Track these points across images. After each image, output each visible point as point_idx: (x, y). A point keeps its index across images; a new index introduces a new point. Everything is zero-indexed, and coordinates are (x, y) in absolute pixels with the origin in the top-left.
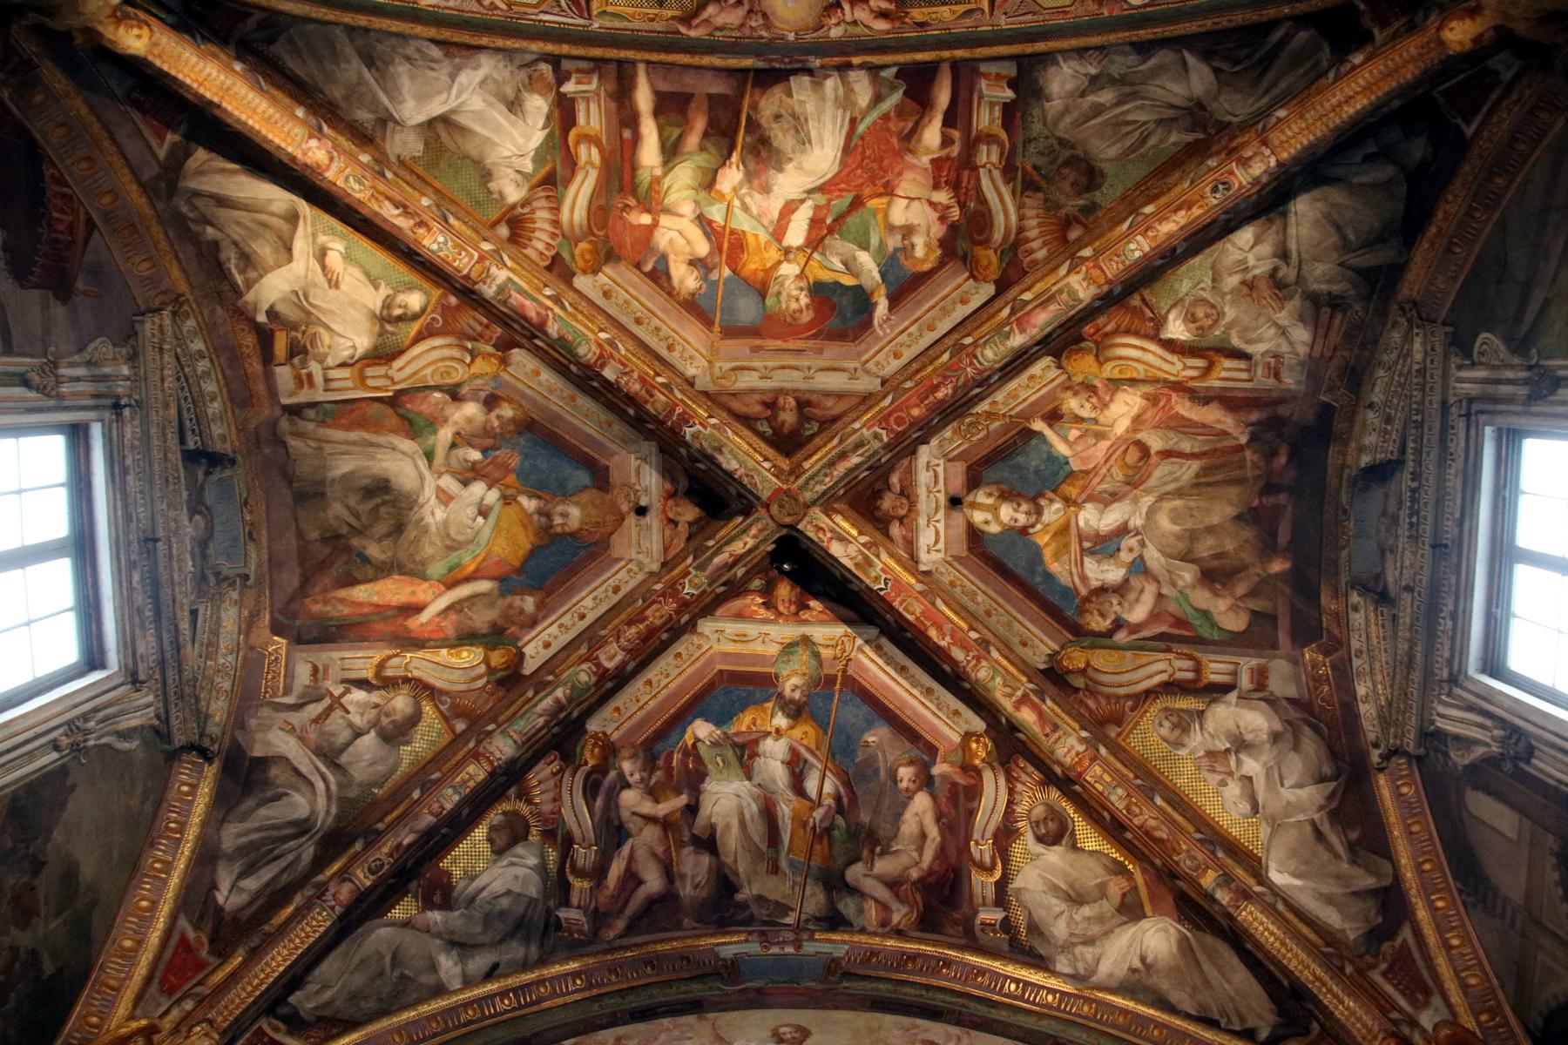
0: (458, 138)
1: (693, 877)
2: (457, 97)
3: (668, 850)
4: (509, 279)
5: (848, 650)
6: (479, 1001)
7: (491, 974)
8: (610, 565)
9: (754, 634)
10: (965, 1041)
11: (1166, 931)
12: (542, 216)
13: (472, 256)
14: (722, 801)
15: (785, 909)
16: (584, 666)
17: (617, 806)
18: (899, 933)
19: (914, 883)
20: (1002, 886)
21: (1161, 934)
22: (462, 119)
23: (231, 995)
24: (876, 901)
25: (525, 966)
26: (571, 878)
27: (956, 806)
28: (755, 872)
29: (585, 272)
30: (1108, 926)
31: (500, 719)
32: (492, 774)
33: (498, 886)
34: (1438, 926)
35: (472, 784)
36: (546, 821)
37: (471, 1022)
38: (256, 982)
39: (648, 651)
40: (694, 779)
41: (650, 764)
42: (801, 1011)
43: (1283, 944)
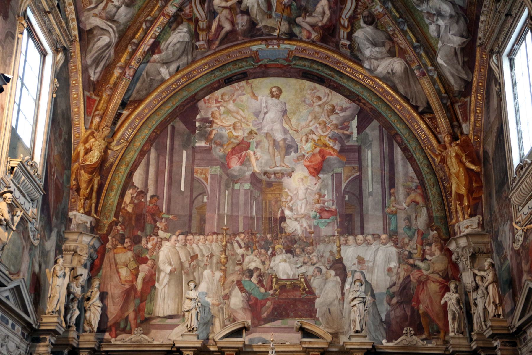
1: (241, 23)
3: (232, 17)
10: (330, 97)
11: (401, 64)
15: (274, 29)
18: (313, 43)
19: (320, 27)
21: (400, 64)
24: (306, 29)
25: (188, 65)
27: (337, 5)
30: (383, 56)
33: (175, 41)
34: (476, 104)
37: (175, 89)
43: (430, 94)
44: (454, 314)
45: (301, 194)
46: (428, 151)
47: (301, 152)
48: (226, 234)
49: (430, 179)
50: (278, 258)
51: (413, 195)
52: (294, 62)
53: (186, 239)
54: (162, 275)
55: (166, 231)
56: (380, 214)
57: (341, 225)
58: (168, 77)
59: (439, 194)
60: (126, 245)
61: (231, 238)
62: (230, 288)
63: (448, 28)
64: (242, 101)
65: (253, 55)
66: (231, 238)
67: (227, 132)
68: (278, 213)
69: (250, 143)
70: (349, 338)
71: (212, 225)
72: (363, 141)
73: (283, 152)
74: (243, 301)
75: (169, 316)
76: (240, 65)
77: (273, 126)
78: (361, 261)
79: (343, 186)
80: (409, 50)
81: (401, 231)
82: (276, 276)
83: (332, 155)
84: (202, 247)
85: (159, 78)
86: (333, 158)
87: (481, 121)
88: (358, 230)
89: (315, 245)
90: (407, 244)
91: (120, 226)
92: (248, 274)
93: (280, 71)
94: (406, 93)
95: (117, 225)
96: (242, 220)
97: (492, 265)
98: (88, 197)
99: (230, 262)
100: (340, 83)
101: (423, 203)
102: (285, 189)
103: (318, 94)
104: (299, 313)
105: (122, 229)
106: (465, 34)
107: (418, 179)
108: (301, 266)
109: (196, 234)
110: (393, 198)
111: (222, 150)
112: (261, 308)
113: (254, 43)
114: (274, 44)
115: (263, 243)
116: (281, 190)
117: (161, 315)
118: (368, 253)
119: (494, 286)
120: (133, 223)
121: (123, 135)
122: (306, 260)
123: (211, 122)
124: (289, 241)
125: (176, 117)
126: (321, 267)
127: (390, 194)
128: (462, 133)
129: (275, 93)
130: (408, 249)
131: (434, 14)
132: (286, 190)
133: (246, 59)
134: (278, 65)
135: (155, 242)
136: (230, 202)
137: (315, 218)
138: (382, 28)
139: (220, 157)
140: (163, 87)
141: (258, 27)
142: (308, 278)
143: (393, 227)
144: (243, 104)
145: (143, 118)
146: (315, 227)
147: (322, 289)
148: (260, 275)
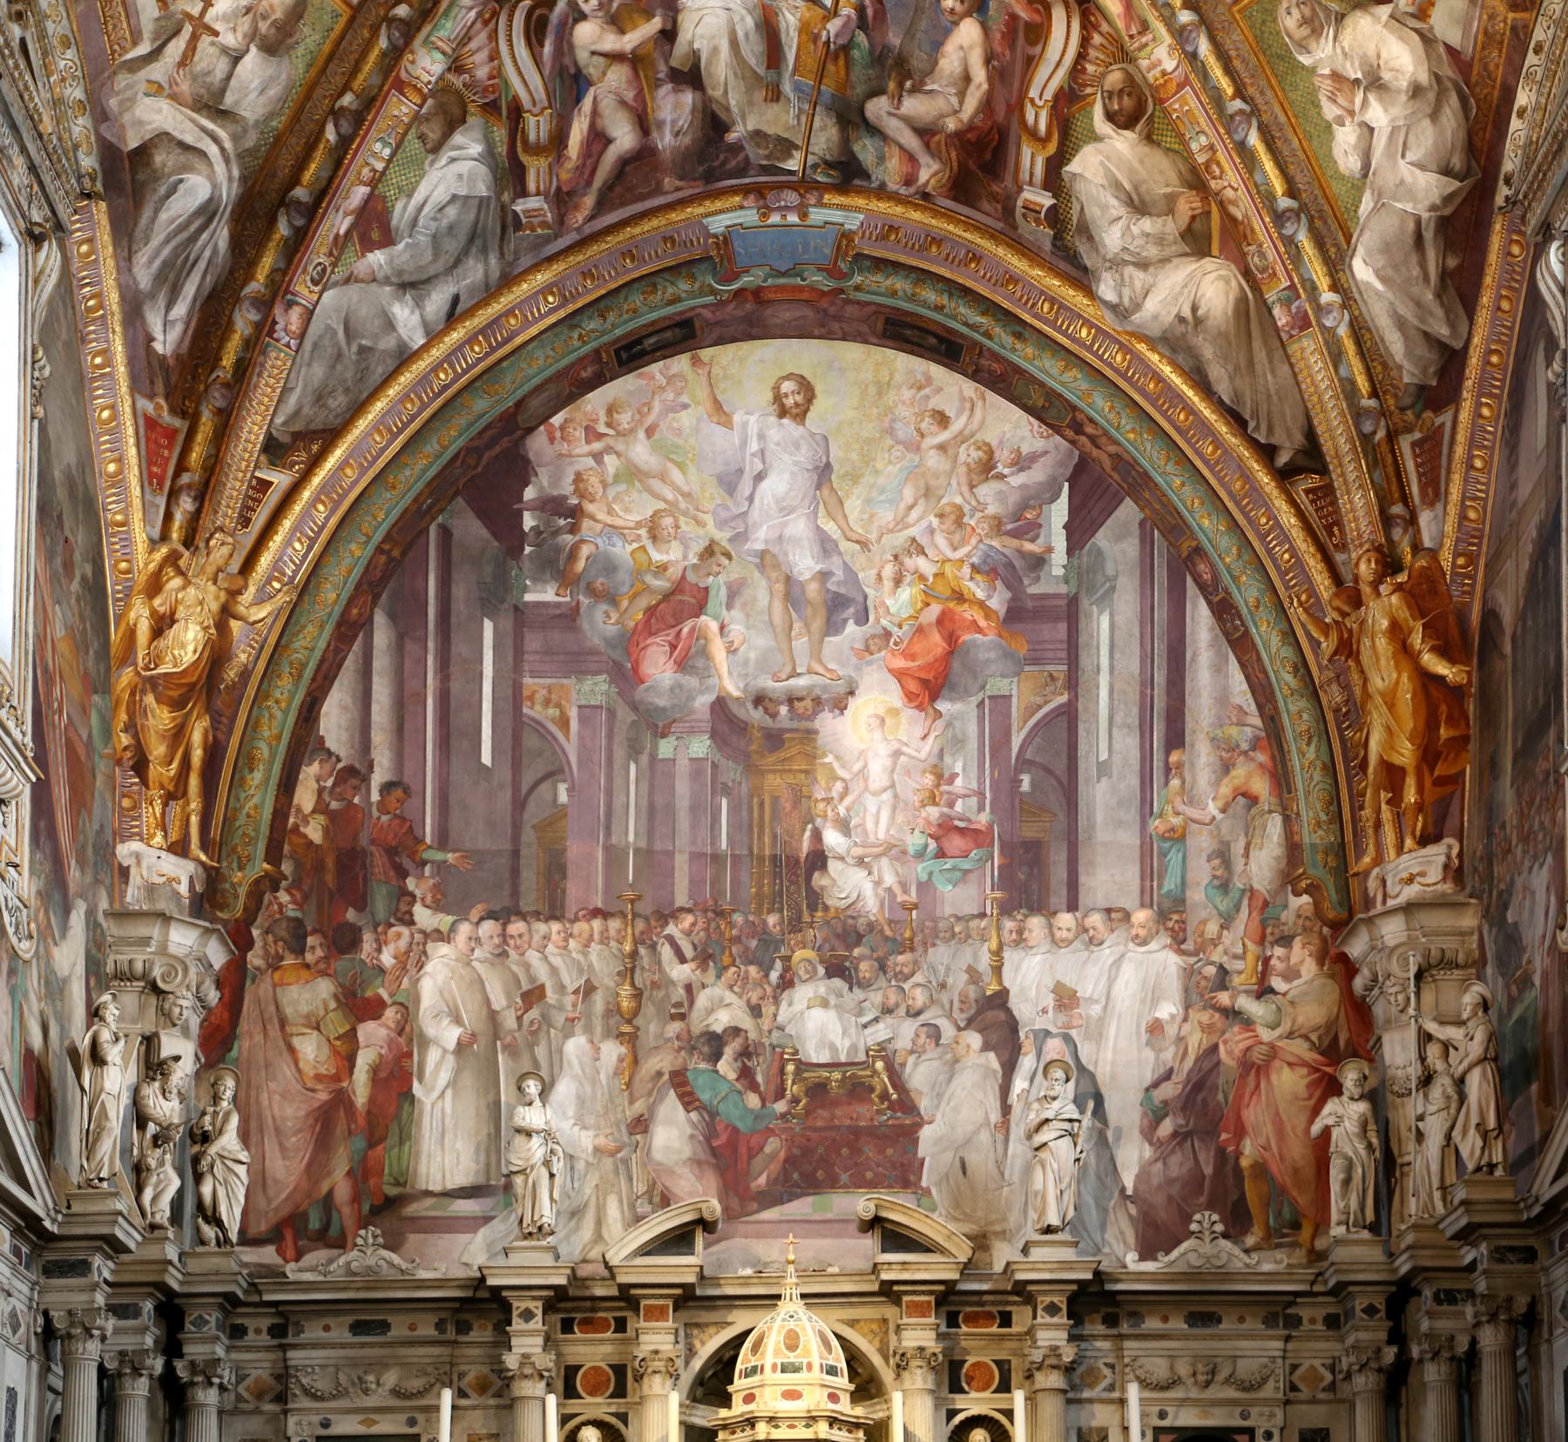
6: (448, 358)
20: (1055, 165)
44: (1349, 1169)
45: (878, 772)
46: (1297, 613)
47: (877, 620)
48: (635, 915)
49: (1299, 714)
50: (802, 994)
51: (1240, 772)
53: (504, 936)
54: (433, 1055)
55: (438, 906)
56: (1129, 838)
57: (1006, 879)
59: (1325, 768)
60: (309, 957)
61: (648, 930)
62: (650, 1094)
63: (1400, 141)
64: (679, 432)
66: (648, 930)
67: (629, 548)
68: (800, 841)
69: (706, 589)
70: (1025, 1251)
71: (587, 882)
72: (1088, 577)
73: (818, 624)
74: (692, 1137)
75: (462, 1189)
77: (785, 525)
78: (1066, 999)
79: (1016, 741)
80: (1260, 227)
81: (1196, 896)
82: (796, 1052)
83: (979, 630)
84: (557, 961)
86: (984, 641)
87: (1485, 500)
88: (1058, 897)
89: (920, 949)
90: (1215, 943)
91: (288, 890)
92: (706, 1049)
93: (809, 313)
94: (1237, 396)
95: (276, 889)
96: (686, 868)
97: (1485, 1005)
98: (175, 793)
99: (649, 1009)
100: (1014, 358)
101: (1274, 800)
102: (825, 755)
103: (936, 403)
104: (869, 1175)
105: (294, 902)
106: (1457, 162)
107: (1261, 716)
108: (876, 1020)
109: (537, 915)
110: (1175, 783)
111: (614, 616)
112: (751, 1157)
113: (718, 205)
114: (786, 208)
115: (754, 943)
116: (812, 757)
117: (436, 1187)
118: (1087, 973)
119: (1484, 1073)
120: (330, 878)
121: (276, 565)
122: (893, 998)
123: (576, 513)
124: (838, 936)
125: (456, 494)
126: (938, 1022)
127: (1168, 769)
128: (1416, 547)
129: (789, 402)
130: (1217, 956)
131: (1357, 82)
132: (829, 759)
135: (403, 944)
136: (644, 802)
137: (920, 855)
138: (1170, 141)
139: (607, 641)
140: (405, 379)
142: (898, 1060)
143: (1170, 884)
144: (680, 442)
146: (921, 886)
147: (940, 1096)
148: (745, 1053)
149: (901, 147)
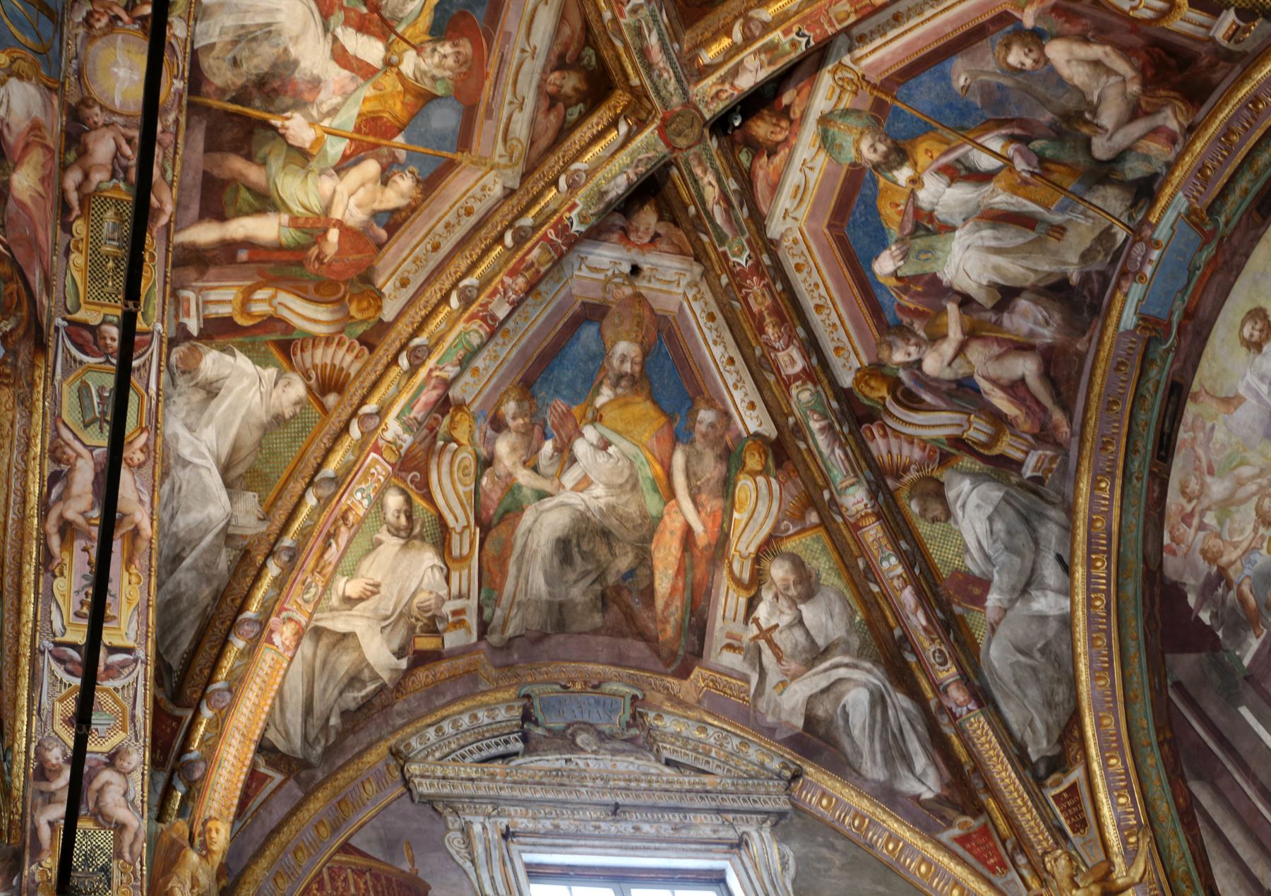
0: (243, 454)
1: (1036, 322)
2: (203, 456)
3: (999, 341)
4: (398, 417)
5: (850, 76)
7: (1066, 567)
8: (685, 318)
9: (801, 175)
12: (321, 356)
13: (375, 461)
14: (968, 268)
15: (1107, 234)
16: (794, 392)
17: (936, 379)
22: (225, 451)
23: (1026, 827)
25: (1069, 530)
26: (996, 451)
28: (1055, 253)
29: (380, 308)
31: (820, 482)
32: (879, 516)
33: (982, 527)
35: (884, 541)
36: (930, 458)
38: (1019, 801)
39: (790, 309)
40: (935, 289)
41: (904, 332)
42: (1232, 294)
52: (1222, 219)
58: (1066, 603)
65: (1148, 334)
76: (1150, 385)
85: (1053, 627)
113: (1115, 313)
114: (1144, 257)
133: (1146, 362)
134: (1203, 274)
141: (1075, 278)
145: (1119, 740)
149: (1142, 137)
